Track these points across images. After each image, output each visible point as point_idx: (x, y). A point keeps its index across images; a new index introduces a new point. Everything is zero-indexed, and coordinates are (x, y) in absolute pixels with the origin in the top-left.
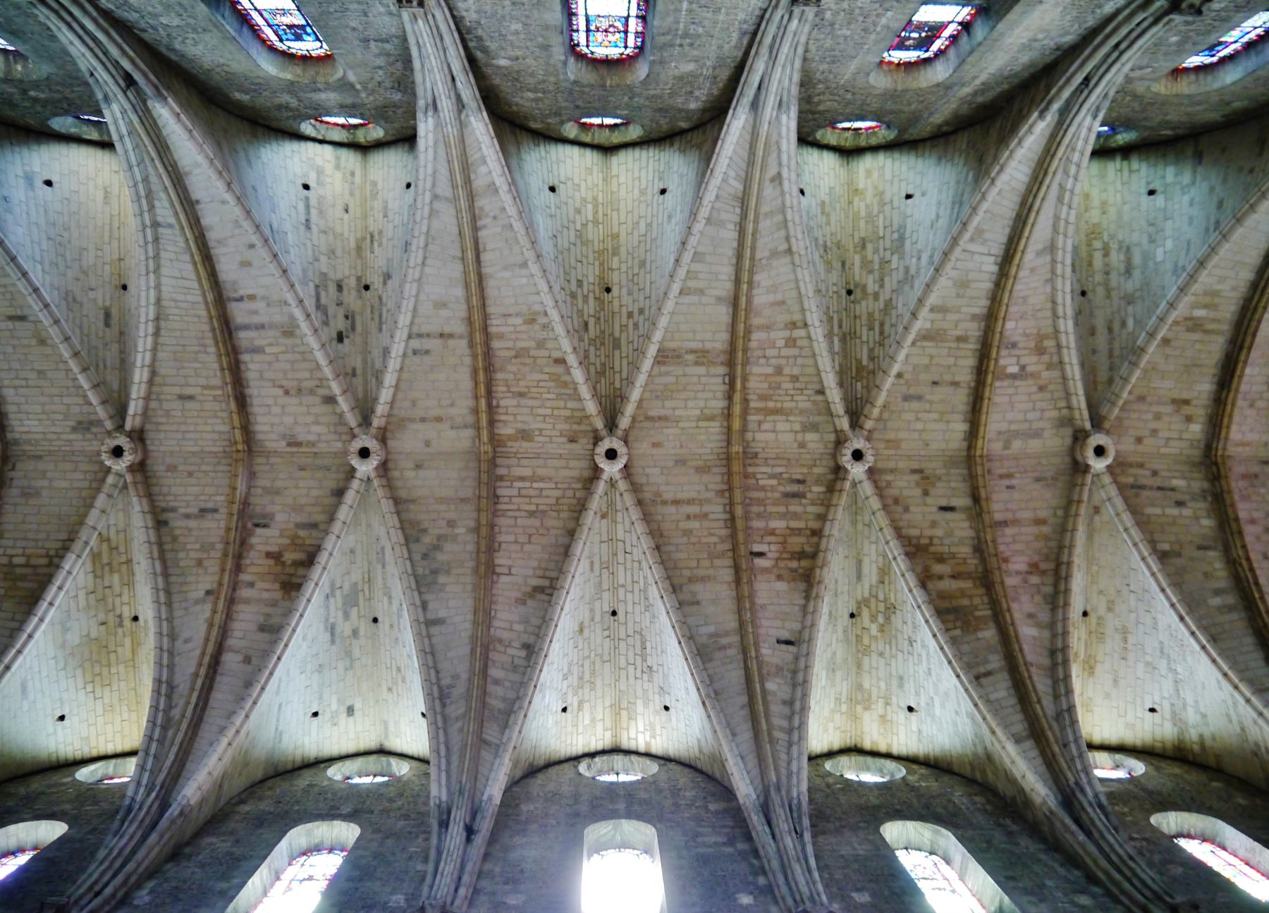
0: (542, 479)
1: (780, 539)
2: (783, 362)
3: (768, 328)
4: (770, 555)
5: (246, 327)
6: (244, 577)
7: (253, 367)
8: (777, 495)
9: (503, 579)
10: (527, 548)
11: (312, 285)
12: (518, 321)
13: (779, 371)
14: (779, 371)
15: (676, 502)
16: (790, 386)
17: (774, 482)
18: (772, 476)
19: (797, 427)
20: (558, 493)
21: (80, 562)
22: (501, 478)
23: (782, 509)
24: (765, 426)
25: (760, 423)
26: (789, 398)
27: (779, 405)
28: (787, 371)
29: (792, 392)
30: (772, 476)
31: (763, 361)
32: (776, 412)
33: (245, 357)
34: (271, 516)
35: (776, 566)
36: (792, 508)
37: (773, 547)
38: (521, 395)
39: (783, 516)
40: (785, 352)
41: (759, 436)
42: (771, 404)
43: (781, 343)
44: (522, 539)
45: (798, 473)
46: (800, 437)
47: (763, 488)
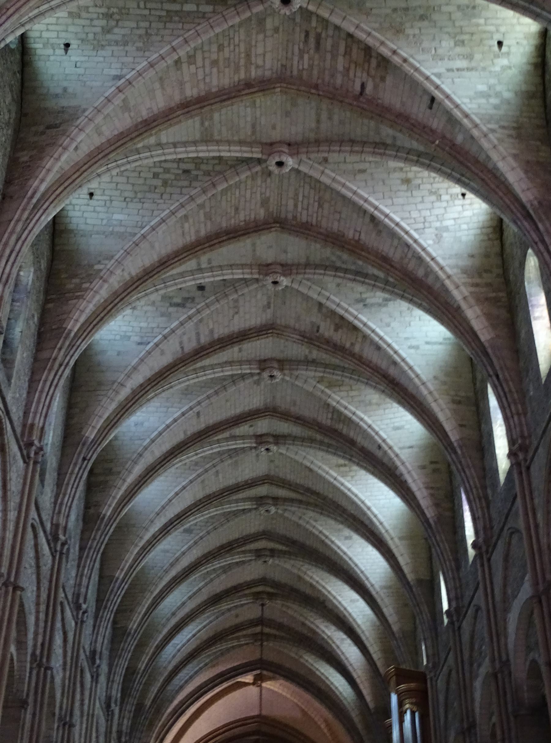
0: (297, 195)
1: (353, 66)
2: (207, 62)
3: (181, 84)
4: (364, 80)
5: (198, 340)
6: (348, 345)
7: (221, 331)
8: (317, 56)
9: (363, 237)
10: (343, 216)
11: (171, 309)
12: (186, 225)
13: (215, 63)
14: (215, 63)
15: (318, 121)
16: (226, 50)
17: (306, 56)
18: (301, 57)
19: (261, 37)
20: (307, 187)
21: (333, 395)
22: (295, 218)
23: (329, 56)
24: (260, 62)
25: (257, 67)
26: (237, 48)
27: (243, 55)
28: (214, 56)
29: (232, 47)
30: (301, 57)
31: (208, 80)
32: (248, 56)
33: (216, 336)
34: (313, 324)
35: (373, 77)
36: (329, 48)
37: (359, 74)
38: (237, 209)
39: (334, 57)
40: (199, 63)
41: (268, 66)
42: (242, 62)
43: (193, 68)
44: (337, 216)
45: (299, 36)
46: (269, 33)
47: (311, 66)
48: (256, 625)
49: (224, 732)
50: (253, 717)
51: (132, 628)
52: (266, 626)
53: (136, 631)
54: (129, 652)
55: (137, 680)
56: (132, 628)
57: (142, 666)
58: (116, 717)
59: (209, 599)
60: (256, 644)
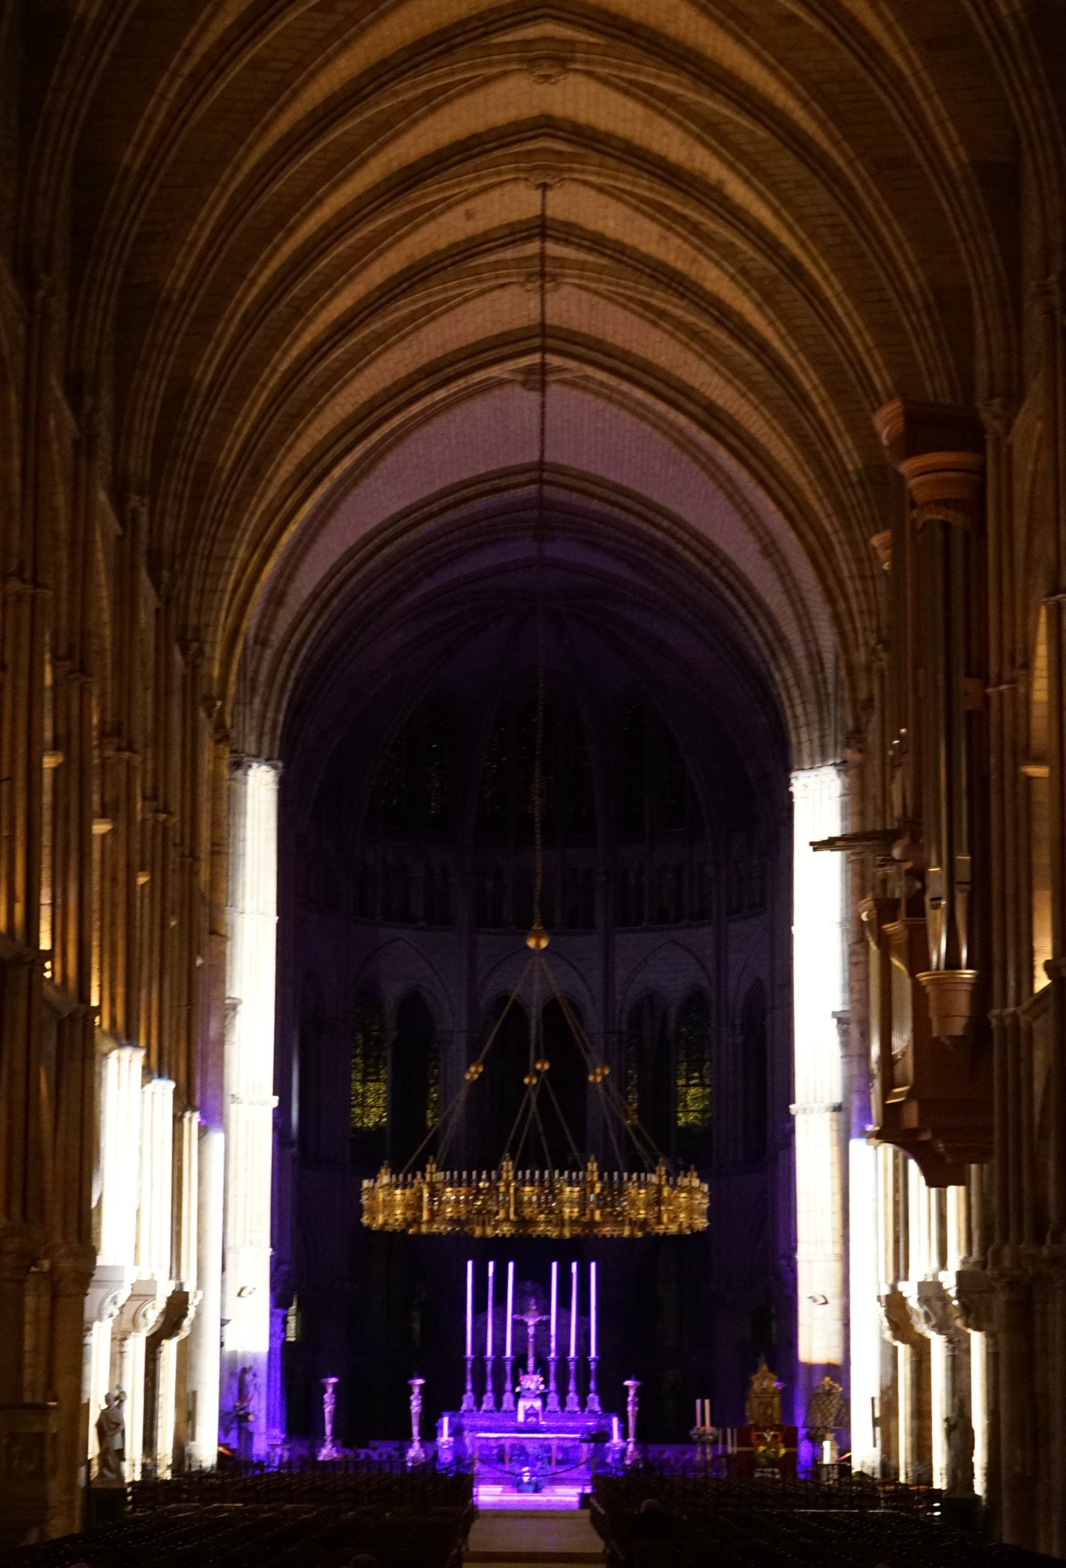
48: (528, 239)
49: (443, 510)
50: (524, 469)
51: (172, 289)
52: (557, 240)
53: (184, 295)
54: (168, 353)
55: (195, 413)
56: (172, 289)
57: (204, 374)
58: (144, 511)
59: (387, 179)
60: (529, 286)
